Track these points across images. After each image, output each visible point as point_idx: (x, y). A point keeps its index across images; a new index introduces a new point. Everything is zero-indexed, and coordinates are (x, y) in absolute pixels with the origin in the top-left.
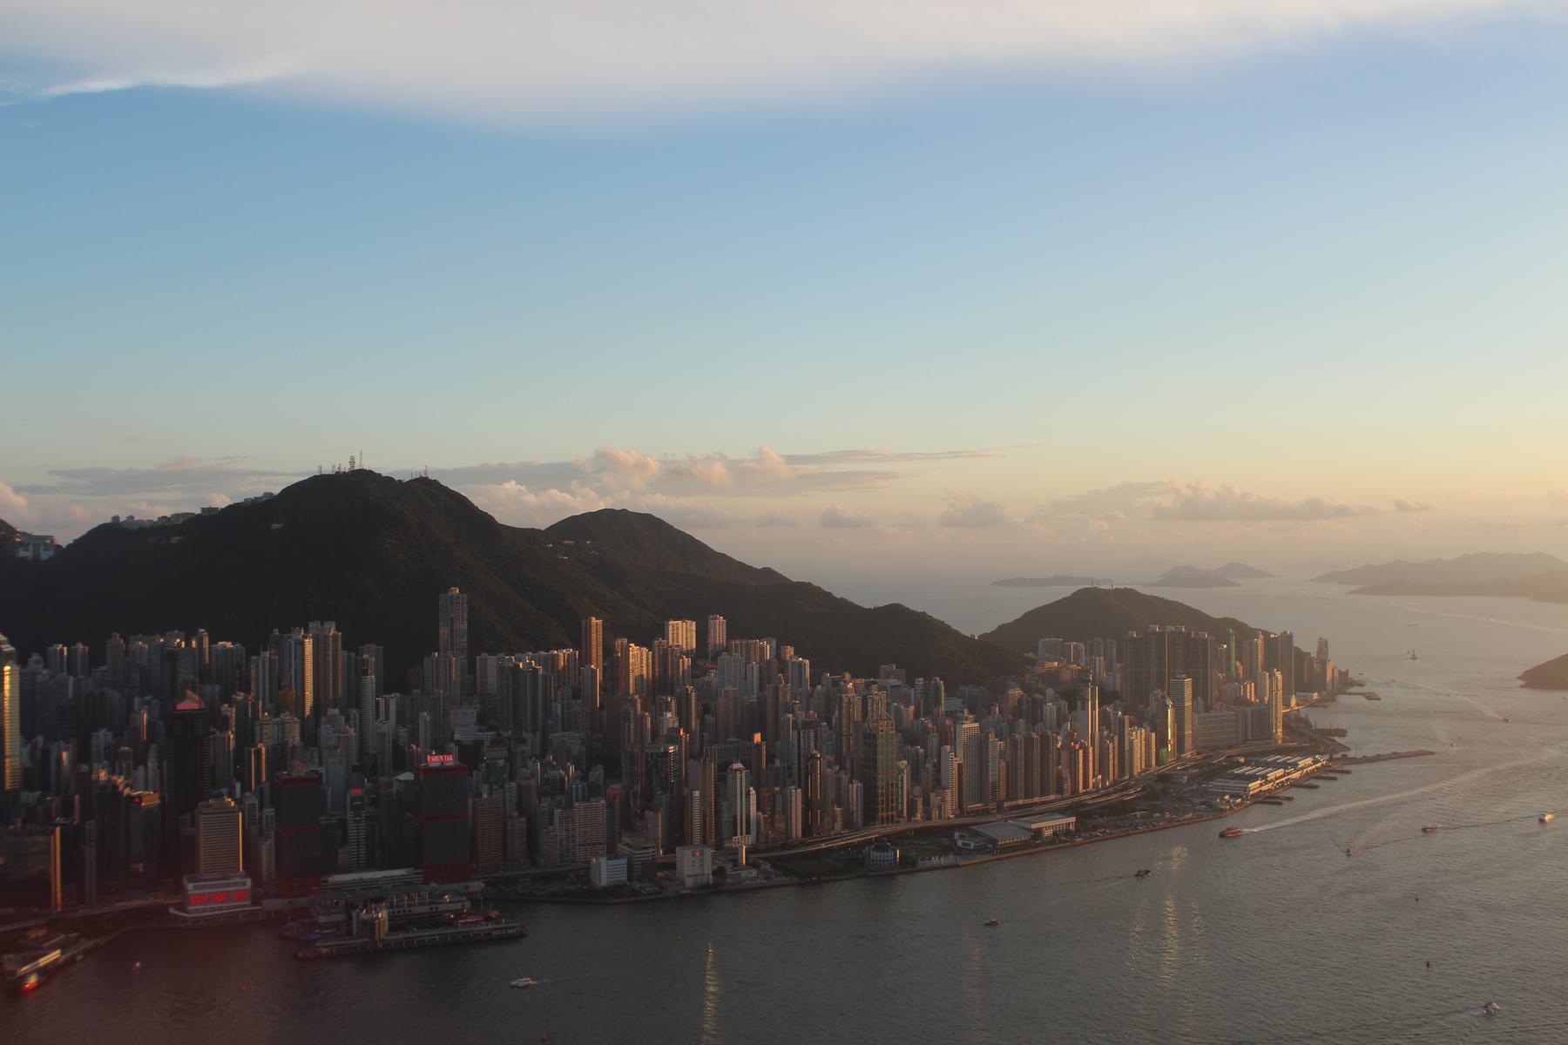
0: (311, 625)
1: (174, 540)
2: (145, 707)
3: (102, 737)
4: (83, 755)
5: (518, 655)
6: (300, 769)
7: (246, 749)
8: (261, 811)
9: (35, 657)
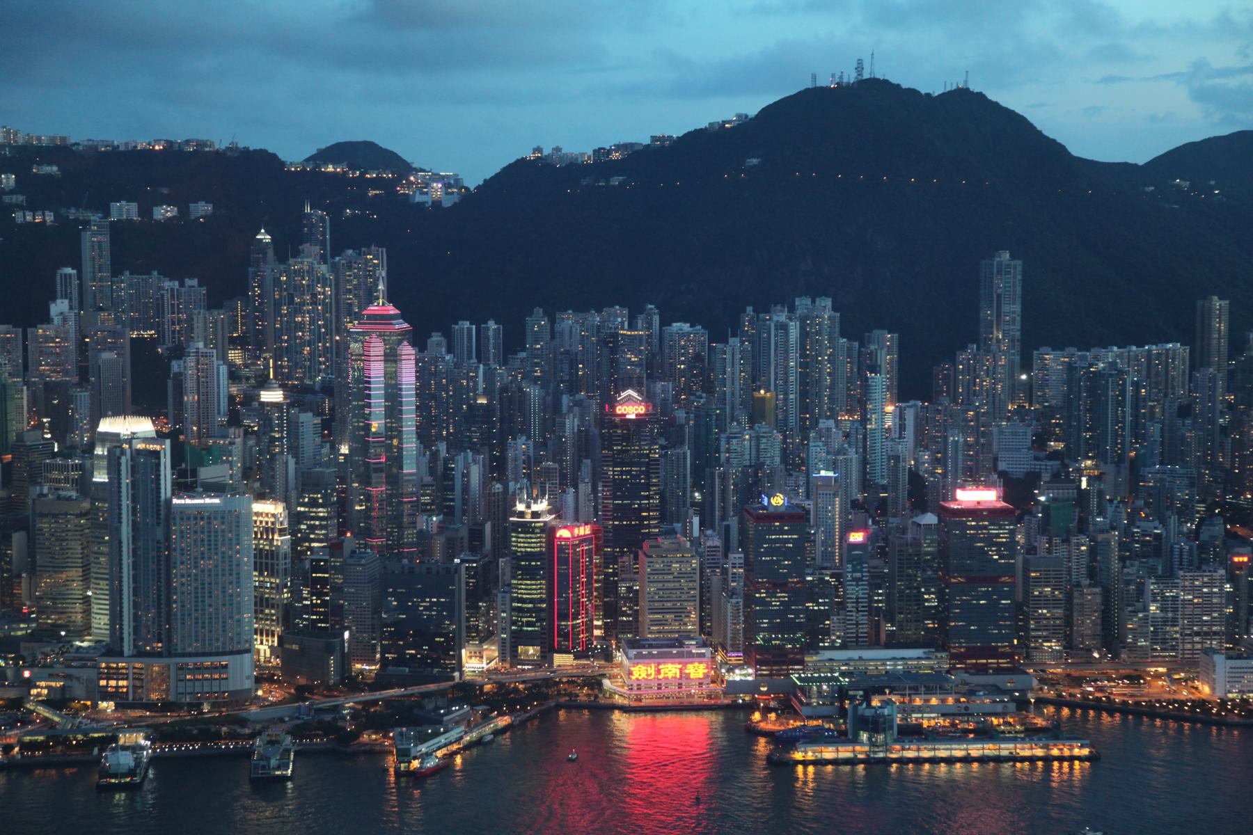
0: (797, 301)
1: (615, 181)
2: (576, 409)
3: (521, 446)
4: (497, 468)
5: (1095, 351)
6: (778, 500)
7: (707, 470)
8: (726, 556)
9: (436, 338)
